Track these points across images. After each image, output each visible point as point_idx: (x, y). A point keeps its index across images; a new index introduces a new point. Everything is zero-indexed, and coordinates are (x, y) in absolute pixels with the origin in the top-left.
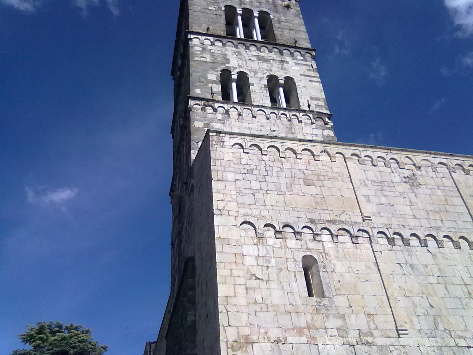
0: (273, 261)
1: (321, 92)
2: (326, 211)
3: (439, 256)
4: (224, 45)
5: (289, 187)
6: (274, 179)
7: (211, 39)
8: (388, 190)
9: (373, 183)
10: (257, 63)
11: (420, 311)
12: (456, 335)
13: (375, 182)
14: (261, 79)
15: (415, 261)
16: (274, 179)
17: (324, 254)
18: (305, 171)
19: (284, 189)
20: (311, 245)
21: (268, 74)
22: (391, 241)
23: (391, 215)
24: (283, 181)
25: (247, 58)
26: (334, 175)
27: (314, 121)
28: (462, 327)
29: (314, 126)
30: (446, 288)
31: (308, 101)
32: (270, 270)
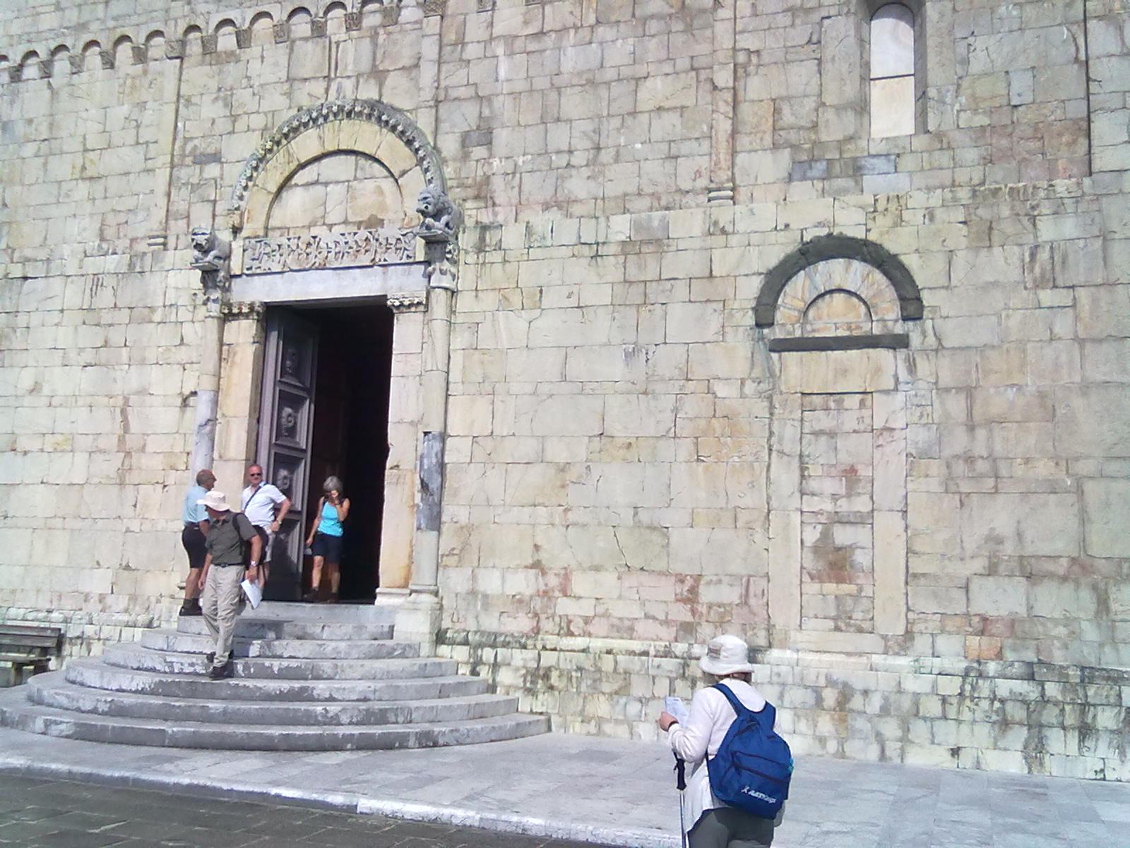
3: (64, 95)
12: (20, 257)
15: (15, 115)
23: (16, 14)
28: (38, 240)
30: (45, 164)
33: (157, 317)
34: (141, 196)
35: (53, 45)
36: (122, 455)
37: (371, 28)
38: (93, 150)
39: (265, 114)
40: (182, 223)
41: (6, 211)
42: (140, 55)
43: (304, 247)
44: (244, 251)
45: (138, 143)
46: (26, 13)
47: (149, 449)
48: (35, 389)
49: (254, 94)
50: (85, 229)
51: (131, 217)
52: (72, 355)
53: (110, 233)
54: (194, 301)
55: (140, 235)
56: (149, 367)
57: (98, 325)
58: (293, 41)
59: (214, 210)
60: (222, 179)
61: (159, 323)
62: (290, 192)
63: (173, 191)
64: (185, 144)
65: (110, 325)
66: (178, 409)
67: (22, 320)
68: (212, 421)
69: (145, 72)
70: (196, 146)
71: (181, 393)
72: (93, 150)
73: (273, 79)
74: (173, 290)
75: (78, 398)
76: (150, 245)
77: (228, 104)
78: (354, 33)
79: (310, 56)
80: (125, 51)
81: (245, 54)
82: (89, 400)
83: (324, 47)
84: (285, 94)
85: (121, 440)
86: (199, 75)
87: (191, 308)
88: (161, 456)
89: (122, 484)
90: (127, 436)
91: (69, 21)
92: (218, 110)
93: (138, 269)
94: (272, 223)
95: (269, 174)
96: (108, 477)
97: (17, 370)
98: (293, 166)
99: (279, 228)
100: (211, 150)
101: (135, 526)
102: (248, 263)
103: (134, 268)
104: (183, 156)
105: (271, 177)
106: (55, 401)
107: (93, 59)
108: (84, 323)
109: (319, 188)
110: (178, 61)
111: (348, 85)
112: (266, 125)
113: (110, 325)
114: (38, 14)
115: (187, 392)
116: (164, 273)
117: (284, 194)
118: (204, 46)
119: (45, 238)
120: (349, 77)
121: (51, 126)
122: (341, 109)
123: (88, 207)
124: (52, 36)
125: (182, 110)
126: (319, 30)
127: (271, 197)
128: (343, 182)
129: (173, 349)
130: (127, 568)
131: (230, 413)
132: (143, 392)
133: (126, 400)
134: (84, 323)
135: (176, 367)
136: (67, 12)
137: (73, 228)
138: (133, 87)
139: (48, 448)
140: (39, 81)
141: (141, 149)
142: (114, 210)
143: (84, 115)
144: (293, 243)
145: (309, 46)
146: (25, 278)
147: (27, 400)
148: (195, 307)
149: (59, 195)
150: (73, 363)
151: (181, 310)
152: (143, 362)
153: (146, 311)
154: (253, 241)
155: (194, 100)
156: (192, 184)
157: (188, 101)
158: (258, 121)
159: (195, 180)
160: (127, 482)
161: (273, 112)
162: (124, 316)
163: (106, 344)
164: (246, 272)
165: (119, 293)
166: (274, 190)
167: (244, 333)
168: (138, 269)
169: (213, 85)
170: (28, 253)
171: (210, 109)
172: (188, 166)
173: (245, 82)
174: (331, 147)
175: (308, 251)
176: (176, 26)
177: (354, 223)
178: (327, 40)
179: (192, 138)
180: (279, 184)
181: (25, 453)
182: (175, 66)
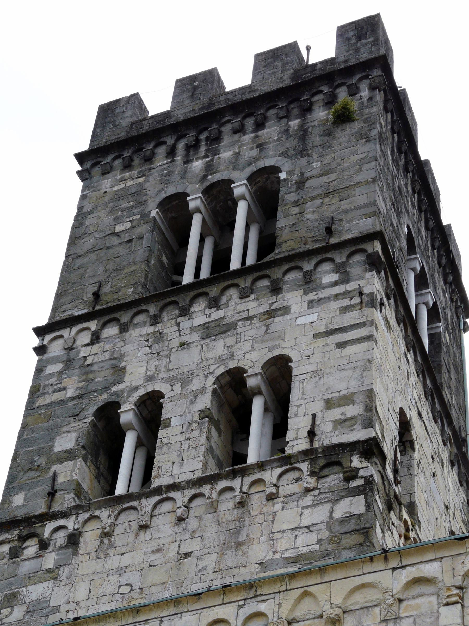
4: (124, 329)
7: (93, 325)
10: (199, 347)
14: (196, 395)
21: (222, 370)
25: (175, 343)
27: (311, 482)
29: (309, 500)
31: (314, 416)
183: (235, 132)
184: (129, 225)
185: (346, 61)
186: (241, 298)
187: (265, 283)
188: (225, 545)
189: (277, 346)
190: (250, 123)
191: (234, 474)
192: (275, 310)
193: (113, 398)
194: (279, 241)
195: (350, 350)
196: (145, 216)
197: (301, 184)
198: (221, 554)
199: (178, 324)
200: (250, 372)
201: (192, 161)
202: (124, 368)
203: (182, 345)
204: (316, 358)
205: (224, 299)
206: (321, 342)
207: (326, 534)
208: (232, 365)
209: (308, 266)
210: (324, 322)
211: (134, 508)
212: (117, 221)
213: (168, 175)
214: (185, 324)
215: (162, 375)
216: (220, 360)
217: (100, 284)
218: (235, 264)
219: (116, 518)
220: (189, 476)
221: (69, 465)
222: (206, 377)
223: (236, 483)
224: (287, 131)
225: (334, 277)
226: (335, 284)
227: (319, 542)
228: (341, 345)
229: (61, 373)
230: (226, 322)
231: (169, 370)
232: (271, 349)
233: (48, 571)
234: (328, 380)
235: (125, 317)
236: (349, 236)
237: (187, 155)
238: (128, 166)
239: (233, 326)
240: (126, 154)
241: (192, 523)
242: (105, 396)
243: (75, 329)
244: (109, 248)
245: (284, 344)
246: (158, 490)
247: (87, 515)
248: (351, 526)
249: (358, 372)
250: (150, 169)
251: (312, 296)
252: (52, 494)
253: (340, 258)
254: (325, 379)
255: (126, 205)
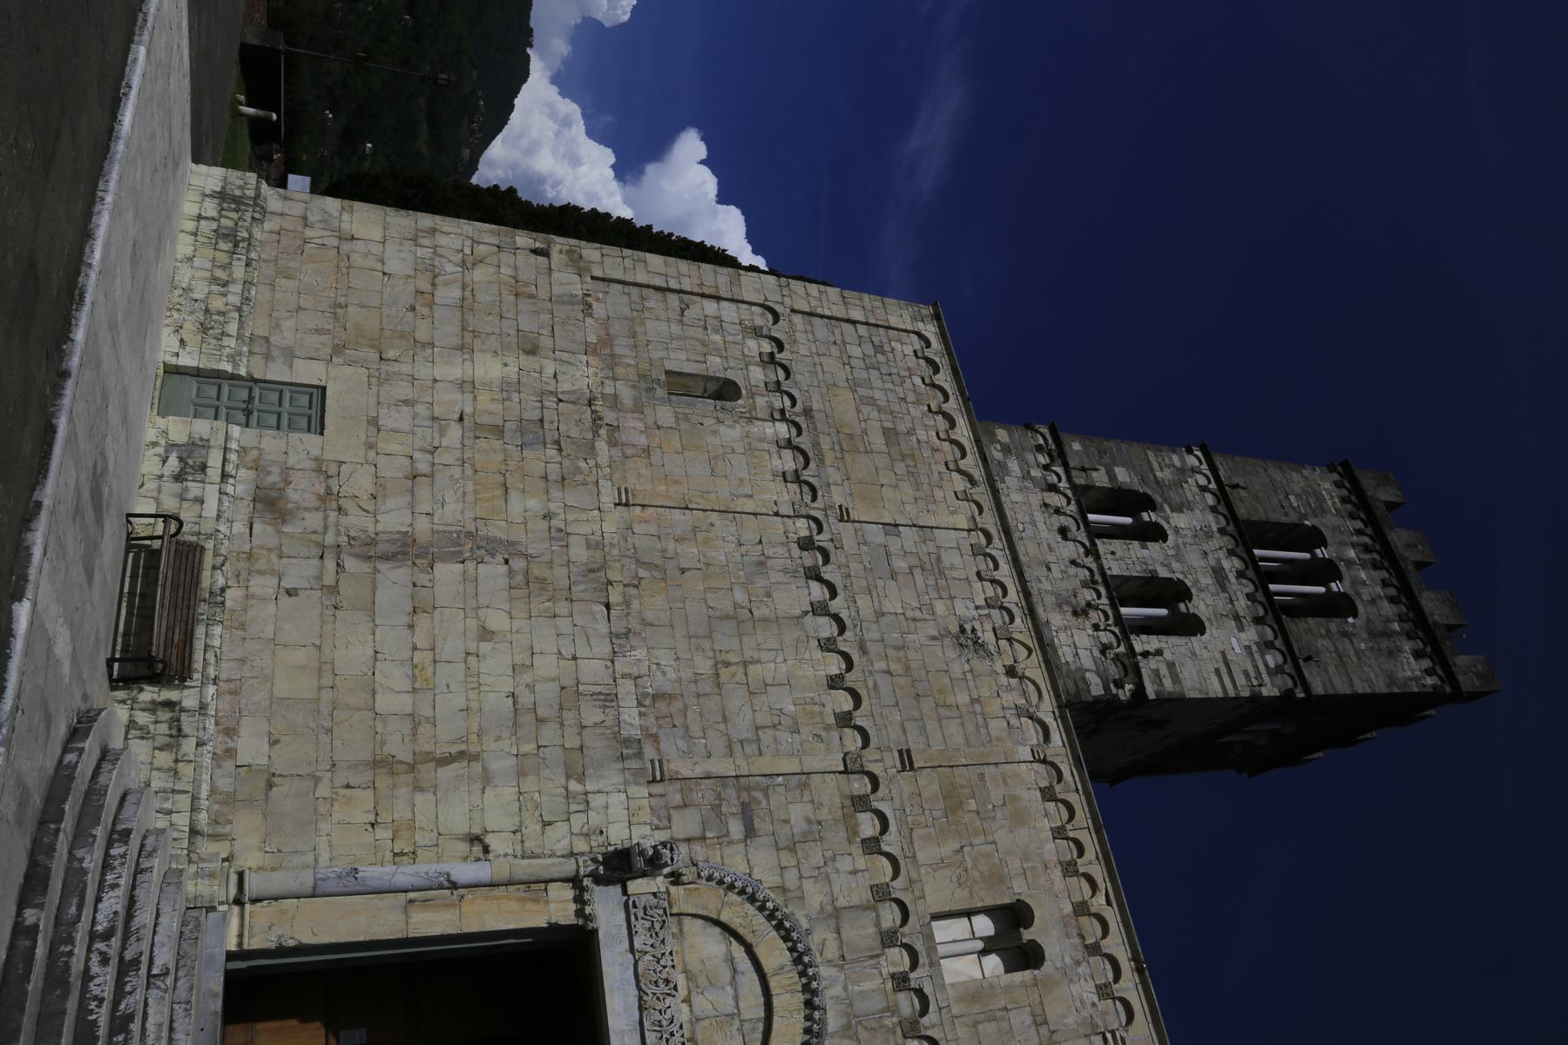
0: (717, 338)
1: (1201, 691)
2: (837, 447)
4: (1213, 509)
5: (871, 401)
6: (877, 383)
7: (1213, 486)
8: (928, 582)
9: (933, 557)
11: (671, 546)
12: (630, 596)
13: (939, 559)
14: (1168, 566)
15: (775, 577)
16: (877, 383)
17: (748, 415)
18: (914, 438)
19: (862, 391)
20: (761, 401)
21: (1189, 584)
22: (806, 544)
23: (869, 566)
24: (877, 394)
25: (1206, 548)
26: (925, 487)
28: (650, 616)
32: (700, 330)
33: (574, 786)
34: (703, 741)
35: (844, 615)
36: (409, 758)
37: (897, 1005)
38: (746, 674)
39: (800, 888)
40: (677, 798)
41: (677, 573)
42: (844, 720)
43: (664, 976)
44: (654, 894)
45: (757, 728)
46: (870, 579)
47: (419, 798)
48: (486, 634)
49: (818, 868)
50: (664, 673)
51: (680, 732)
52: (527, 678)
53: (662, 706)
54: (594, 832)
55: (664, 746)
56: (514, 783)
57: (561, 708)
58: (875, 909)
59: (696, 839)
60: (729, 843)
61: (566, 789)
62: (721, 937)
63: (712, 781)
64: (761, 790)
65: (562, 724)
66: (467, 830)
67: (562, 608)
68: (454, 886)
69: (827, 728)
70: (759, 803)
71: (486, 831)
72: (746, 674)
73: (836, 891)
74: (604, 803)
75: (477, 691)
76: (652, 761)
77: (806, 837)
78: (889, 985)
79: (861, 932)
80: (844, 702)
81: (857, 849)
82: (475, 705)
83: (872, 949)
84: (822, 909)
85: (429, 757)
86: (831, 792)
87: (585, 830)
88: (409, 815)
89: (376, 764)
90: (433, 764)
91: (868, 630)
92: (799, 825)
93: (625, 751)
94: (687, 921)
95: (738, 909)
96: (383, 743)
97: (506, 606)
98: (749, 938)
99: (681, 930)
100: (757, 824)
101: (323, 791)
102: (641, 902)
103: (626, 748)
104: (748, 789)
105: (737, 913)
106: (472, 660)
107: (835, 665)
108: (563, 688)
109: (729, 975)
110: (842, 769)
111: (837, 990)
112: (790, 891)
113: (562, 724)
114: (870, 593)
115: (489, 839)
116: (622, 787)
117: (717, 930)
118: (860, 797)
119: (651, 625)
120: (845, 989)
121: (765, 620)
122: (814, 993)
123: (687, 674)
124: (853, 614)
125: (794, 780)
126: (888, 939)
127: (714, 916)
128: (737, 1007)
129: (537, 814)
130: (270, 785)
131: (466, 907)
132: (487, 779)
133: (475, 757)
134: (563, 688)
135: (517, 819)
136: (875, 626)
137: (665, 658)
138: (812, 713)
139: (418, 657)
140: (808, 599)
141: (750, 735)
142: (686, 707)
143: (780, 659)
144: (666, 961)
145: (872, 930)
146: (608, 606)
147: (472, 623)
148: (587, 835)
149: (698, 637)
150: (518, 678)
151: (583, 816)
152: (521, 773)
153: (580, 770)
154: (666, 904)
155: (806, 793)
156: (720, 805)
157: (804, 786)
158: (791, 879)
159: (724, 809)
160: (378, 771)
161: (802, 898)
162: (572, 741)
163: (540, 721)
164: (632, 899)
165: (599, 731)
166: (724, 918)
167: (558, 908)
168: (625, 751)
169: (824, 814)
170: (635, 605)
171: (798, 813)
172: (739, 797)
173: (829, 854)
174: (773, 983)
175: (661, 982)
176: (876, 761)
177: (693, 1032)
178: (879, 952)
179: (767, 796)
180: (728, 923)
181: (411, 627)
182: (837, 765)
183: (1383, 581)
184: (1295, 505)
185: (1455, 665)
186: (1247, 594)
187: (1261, 612)
188: (1057, 595)
189: (1212, 624)
190: (1392, 591)
191: (1110, 597)
192: (1240, 621)
193: (1158, 506)
194: (1297, 620)
195: (1214, 679)
196: (1305, 516)
197: (1345, 634)
198: (1051, 593)
199: (1221, 548)
200: (1189, 605)
201: (1354, 549)
202: (1183, 512)
203: (1206, 553)
204: (1205, 654)
205: (1244, 581)
206: (1219, 657)
207: (1073, 667)
208: (1193, 591)
209: (1279, 643)
210: (1234, 658)
211: (1079, 529)
212: (1298, 496)
213: (1340, 531)
214: (1222, 554)
215: (1180, 540)
216: (1196, 582)
217: (1244, 488)
218: (1273, 587)
219: (1070, 516)
220: (1106, 565)
221: (1106, 479)
222: (1182, 573)
223: (1105, 600)
224: (1389, 621)
225: (1272, 664)
226: (1266, 665)
227: (1067, 663)
228: (1217, 672)
229: (1173, 466)
230: (1227, 584)
231: (1184, 544)
232: (1209, 619)
233: (1029, 472)
234: (1189, 664)
235: (1221, 509)
236: (1306, 674)
237: (1358, 545)
238: (1344, 500)
239: (1224, 590)
240: (1353, 498)
241: (1072, 570)
242: (1160, 500)
243: (1208, 473)
244: (1275, 492)
245: (1214, 631)
246: (1094, 545)
247: (1070, 495)
248: (1081, 685)
249: (1198, 686)
250: (1343, 517)
251: (1254, 648)
252: (1083, 469)
253: (1288, 668)
254: (1189, 661)
255: (1312, 501)
